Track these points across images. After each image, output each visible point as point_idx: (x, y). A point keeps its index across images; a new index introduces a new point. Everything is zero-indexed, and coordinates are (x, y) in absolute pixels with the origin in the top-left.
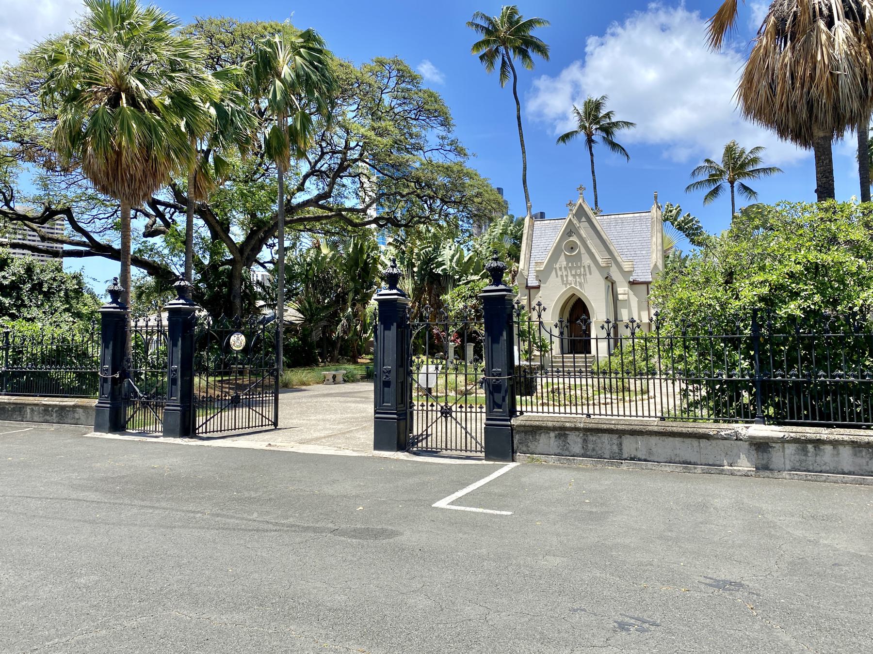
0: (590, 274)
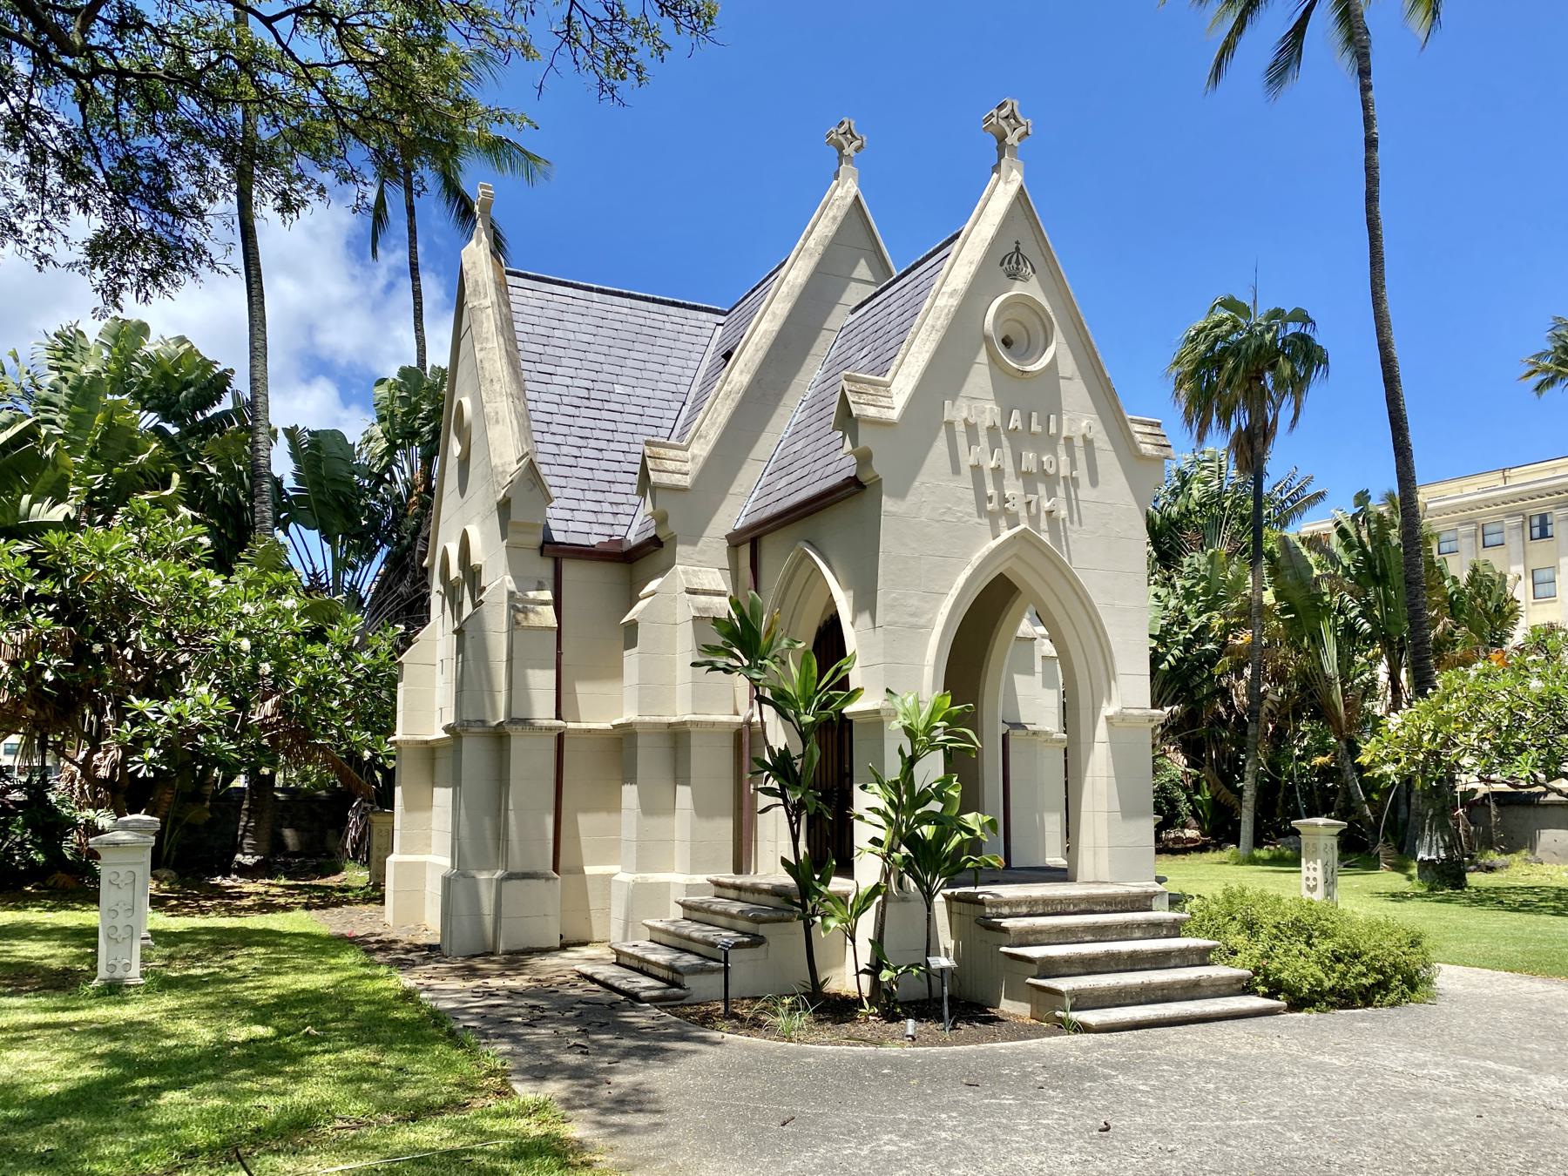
0: (1094, 482)
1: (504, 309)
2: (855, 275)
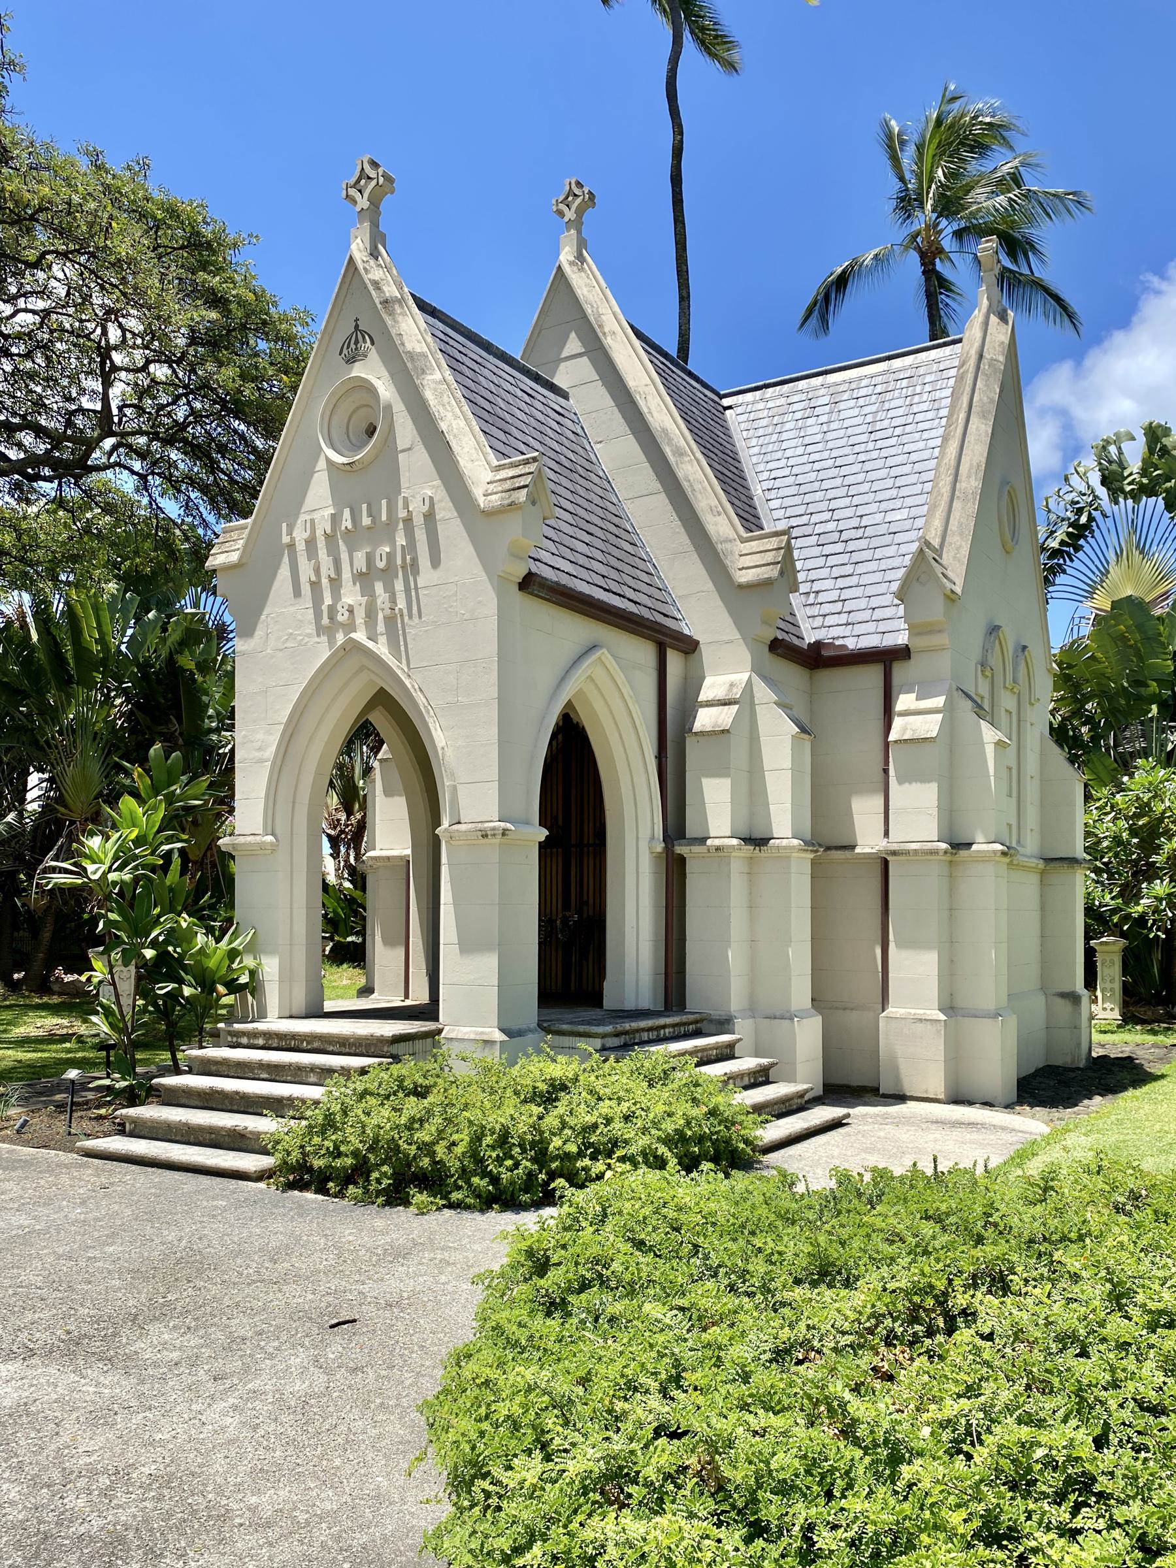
0: (435, 562)
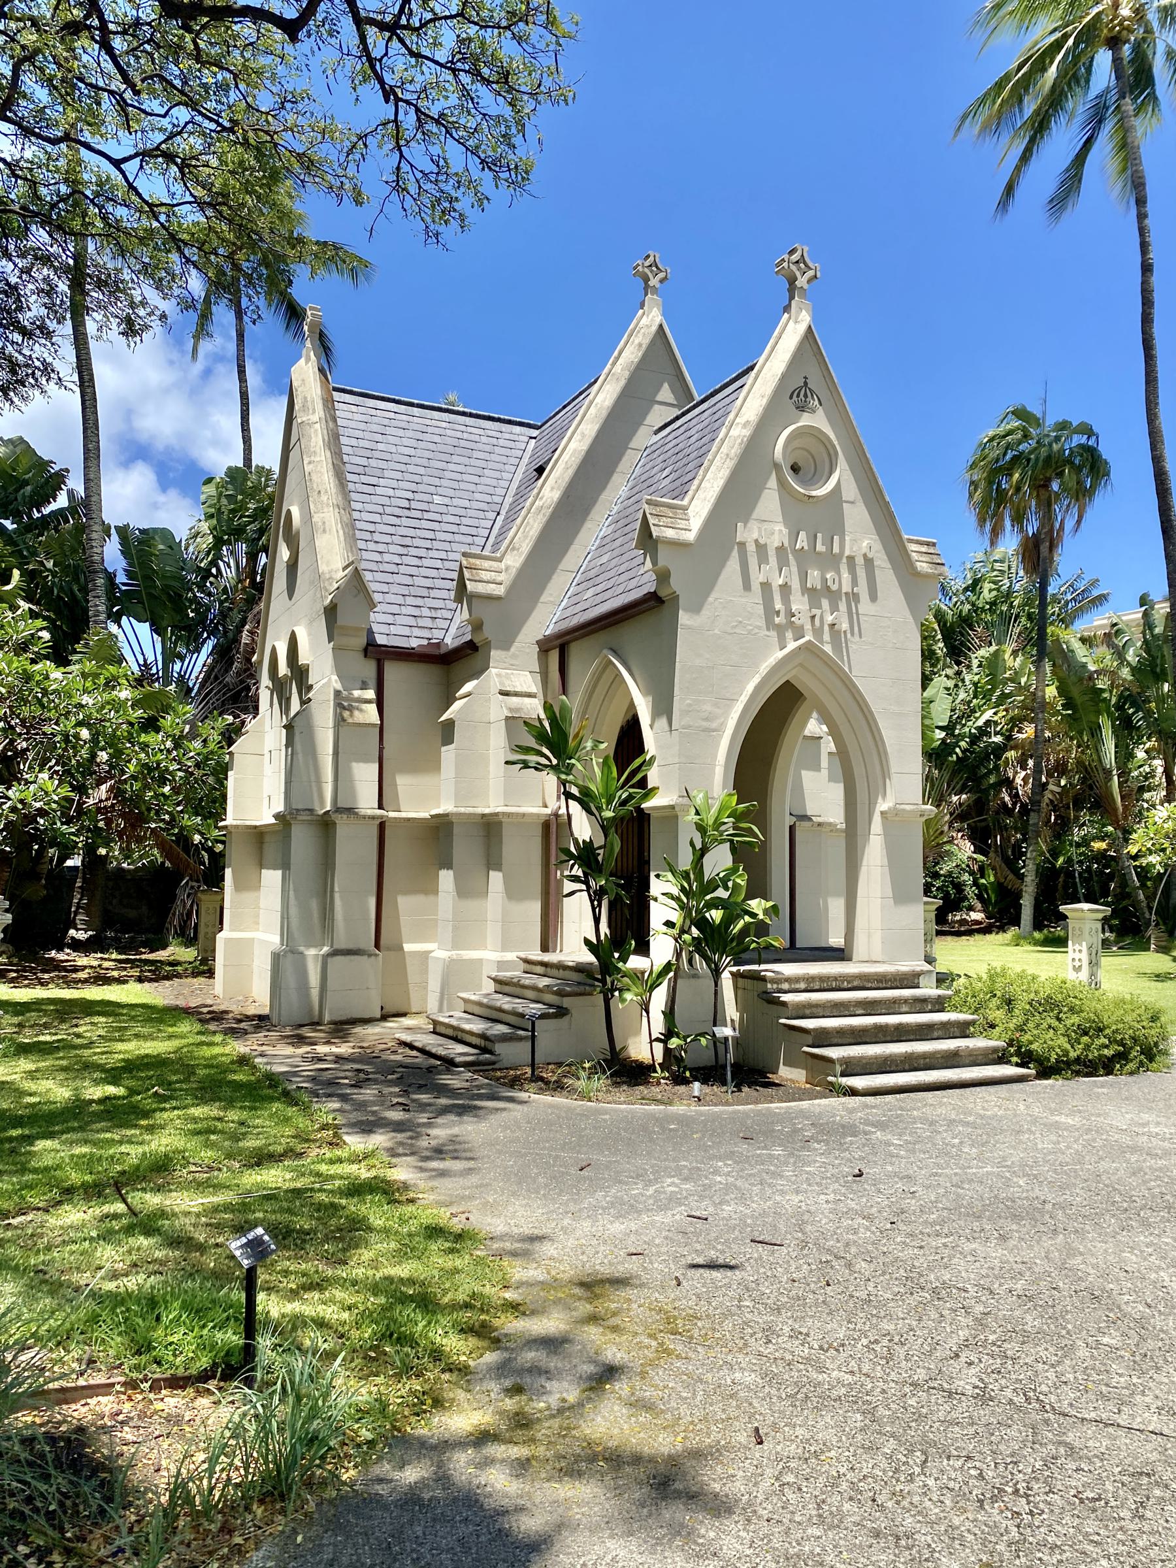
0: (873, 597)
1: (331, 424)
2: (659, 398)
